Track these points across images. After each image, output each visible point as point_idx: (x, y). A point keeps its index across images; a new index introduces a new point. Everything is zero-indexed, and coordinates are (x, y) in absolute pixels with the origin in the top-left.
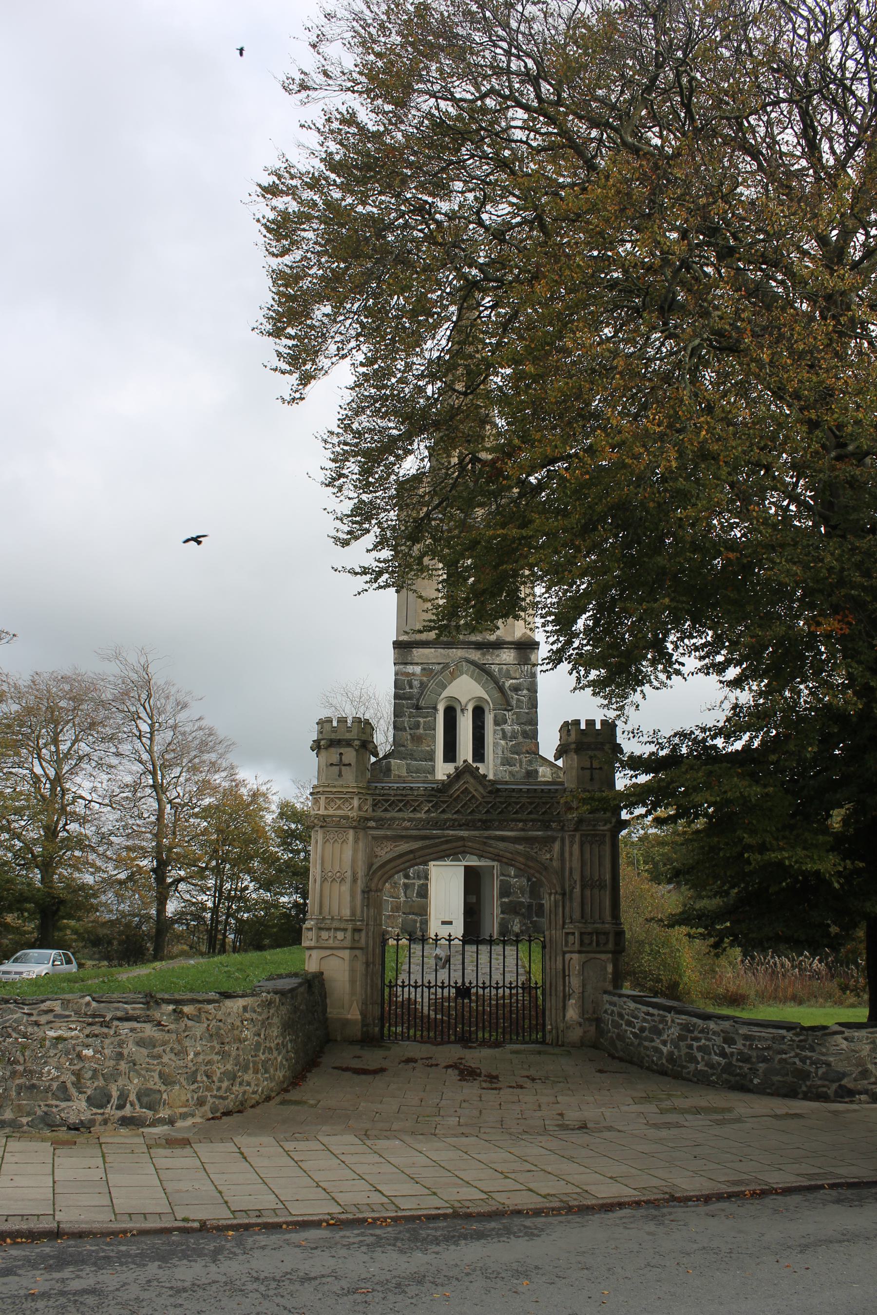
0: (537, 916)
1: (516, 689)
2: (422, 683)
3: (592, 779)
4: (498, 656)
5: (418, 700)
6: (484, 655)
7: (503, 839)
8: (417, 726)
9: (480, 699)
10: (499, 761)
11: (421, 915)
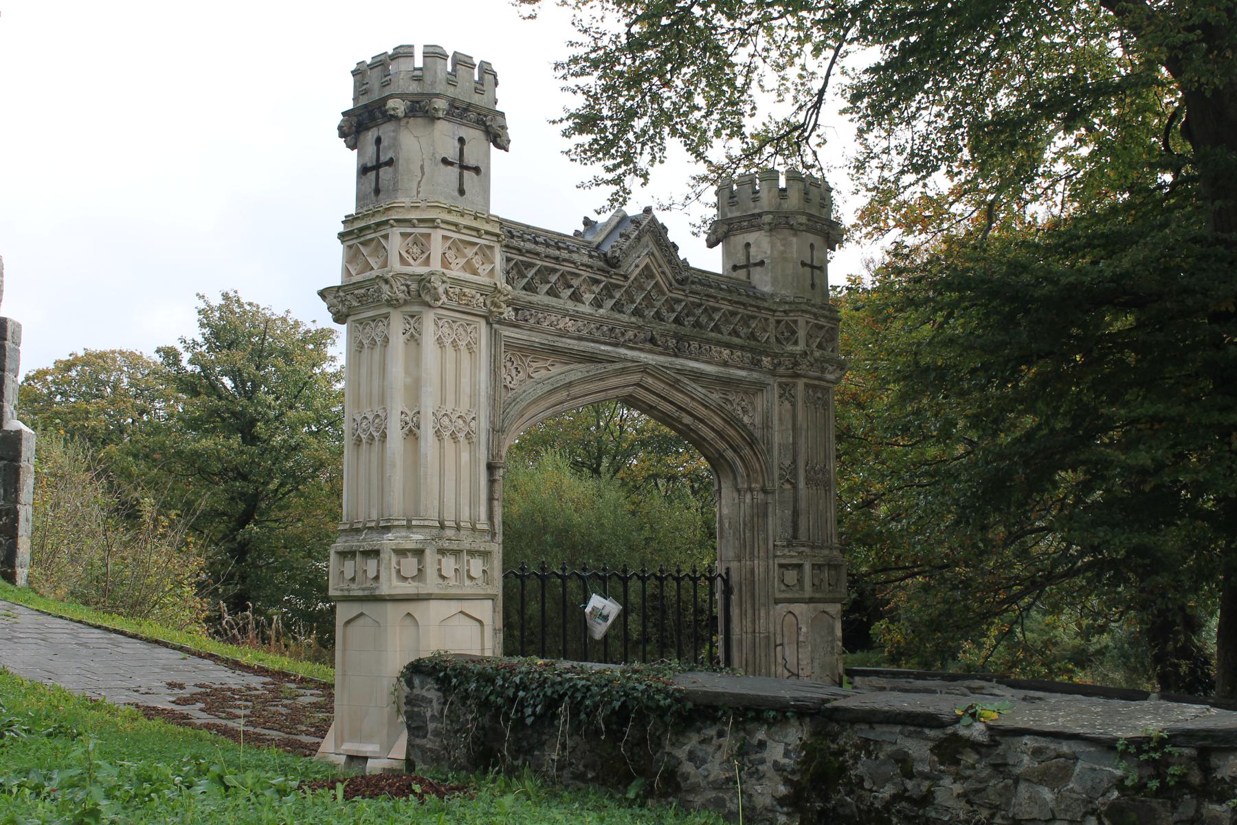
3: (813, 286)
7: (697, 376)
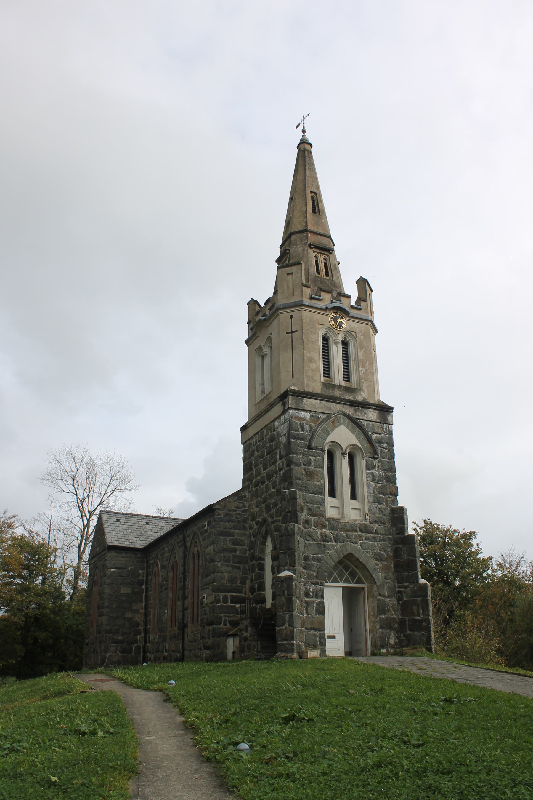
0: (410, 630)
1: (380, 442)
2: (311, 427)
4: (365, 413)
5: (310, 441)
6: (356, 411)
8: (309, 463)
9: (355, 447)
10: (371, 499)
11: (320, 631)
